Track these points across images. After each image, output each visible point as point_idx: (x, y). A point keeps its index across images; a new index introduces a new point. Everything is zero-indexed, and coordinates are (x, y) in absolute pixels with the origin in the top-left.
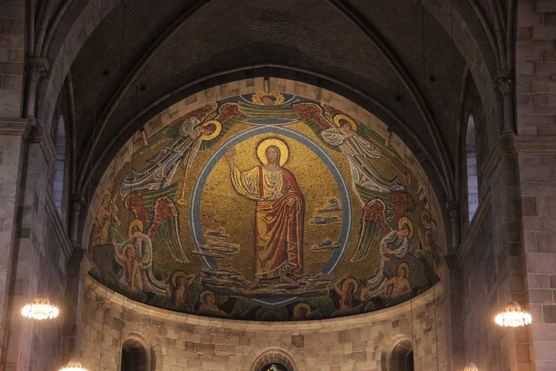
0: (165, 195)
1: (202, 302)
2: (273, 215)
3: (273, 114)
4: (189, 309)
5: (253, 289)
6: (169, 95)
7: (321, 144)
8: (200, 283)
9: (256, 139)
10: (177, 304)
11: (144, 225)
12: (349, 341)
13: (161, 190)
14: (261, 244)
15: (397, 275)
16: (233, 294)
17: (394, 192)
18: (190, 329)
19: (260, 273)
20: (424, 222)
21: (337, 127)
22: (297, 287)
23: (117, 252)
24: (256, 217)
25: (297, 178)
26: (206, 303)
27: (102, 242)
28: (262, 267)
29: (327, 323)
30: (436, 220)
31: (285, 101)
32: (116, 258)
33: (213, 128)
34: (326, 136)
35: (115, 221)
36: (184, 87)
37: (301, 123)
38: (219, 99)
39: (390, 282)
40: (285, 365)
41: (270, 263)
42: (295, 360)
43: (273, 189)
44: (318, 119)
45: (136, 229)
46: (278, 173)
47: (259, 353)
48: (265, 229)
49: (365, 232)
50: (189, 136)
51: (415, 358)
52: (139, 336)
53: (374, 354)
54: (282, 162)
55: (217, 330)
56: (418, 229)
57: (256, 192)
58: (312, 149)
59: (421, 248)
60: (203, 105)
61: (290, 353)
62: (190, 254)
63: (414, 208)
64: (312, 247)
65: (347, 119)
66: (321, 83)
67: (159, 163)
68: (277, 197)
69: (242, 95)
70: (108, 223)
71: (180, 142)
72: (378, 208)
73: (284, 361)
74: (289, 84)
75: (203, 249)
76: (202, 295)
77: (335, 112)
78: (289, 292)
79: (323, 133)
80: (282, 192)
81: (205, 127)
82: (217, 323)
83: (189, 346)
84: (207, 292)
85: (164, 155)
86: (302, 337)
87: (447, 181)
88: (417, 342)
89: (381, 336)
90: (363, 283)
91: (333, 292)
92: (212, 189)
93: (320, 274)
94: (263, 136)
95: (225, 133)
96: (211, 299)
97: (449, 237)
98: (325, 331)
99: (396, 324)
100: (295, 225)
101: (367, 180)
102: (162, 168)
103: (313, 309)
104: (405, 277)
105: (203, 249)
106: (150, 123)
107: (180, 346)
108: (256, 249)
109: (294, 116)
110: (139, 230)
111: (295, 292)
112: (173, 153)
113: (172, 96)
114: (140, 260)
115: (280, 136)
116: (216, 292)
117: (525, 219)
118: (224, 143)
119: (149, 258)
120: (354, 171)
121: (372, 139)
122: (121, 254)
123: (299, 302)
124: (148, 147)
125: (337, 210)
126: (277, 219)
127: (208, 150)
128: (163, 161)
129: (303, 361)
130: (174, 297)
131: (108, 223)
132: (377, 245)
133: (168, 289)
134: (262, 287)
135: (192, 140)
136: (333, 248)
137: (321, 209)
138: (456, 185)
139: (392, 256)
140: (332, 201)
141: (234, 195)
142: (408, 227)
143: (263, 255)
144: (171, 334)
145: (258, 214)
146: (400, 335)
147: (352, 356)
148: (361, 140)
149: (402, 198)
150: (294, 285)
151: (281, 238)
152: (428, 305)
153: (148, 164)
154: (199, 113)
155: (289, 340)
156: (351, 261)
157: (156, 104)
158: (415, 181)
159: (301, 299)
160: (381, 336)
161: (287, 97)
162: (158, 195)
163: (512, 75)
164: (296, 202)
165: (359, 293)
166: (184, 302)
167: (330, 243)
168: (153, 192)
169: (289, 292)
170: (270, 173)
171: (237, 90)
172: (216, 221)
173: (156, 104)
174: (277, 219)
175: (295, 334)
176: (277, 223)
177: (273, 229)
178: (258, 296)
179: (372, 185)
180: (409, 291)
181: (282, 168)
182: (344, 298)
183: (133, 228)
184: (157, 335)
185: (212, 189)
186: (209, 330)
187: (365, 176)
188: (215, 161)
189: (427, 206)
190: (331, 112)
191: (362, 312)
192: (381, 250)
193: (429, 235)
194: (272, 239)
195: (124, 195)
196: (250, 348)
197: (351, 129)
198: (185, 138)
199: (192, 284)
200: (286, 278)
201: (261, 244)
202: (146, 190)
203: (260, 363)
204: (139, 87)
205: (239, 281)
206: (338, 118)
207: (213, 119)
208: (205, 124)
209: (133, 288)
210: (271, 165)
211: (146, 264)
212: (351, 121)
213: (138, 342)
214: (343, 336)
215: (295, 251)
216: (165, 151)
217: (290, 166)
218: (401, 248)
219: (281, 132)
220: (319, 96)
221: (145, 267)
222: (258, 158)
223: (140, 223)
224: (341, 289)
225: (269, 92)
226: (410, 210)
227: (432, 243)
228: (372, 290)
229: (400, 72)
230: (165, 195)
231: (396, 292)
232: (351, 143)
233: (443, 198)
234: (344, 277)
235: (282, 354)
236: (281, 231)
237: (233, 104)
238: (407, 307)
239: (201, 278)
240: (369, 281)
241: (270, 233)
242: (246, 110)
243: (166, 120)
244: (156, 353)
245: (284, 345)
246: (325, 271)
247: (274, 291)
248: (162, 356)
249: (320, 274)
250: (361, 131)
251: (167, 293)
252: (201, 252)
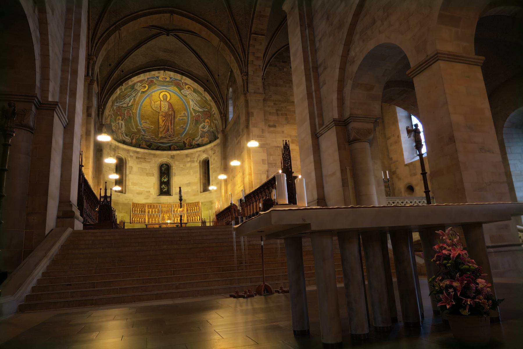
0: (128, 109)
1: (141, 144)
2: (164, 117)
3: (166, 84)
4: (137, 146)
5: (158, 140)
6: (131, 74)
7: (181, 95)
8: (141, 138)
9: (160, 91)
10: (133, 145)
11: (122, 118)
12: (189, 157)
13: (127, 107)
15: (204, 137)
16: (151, 142)
17: (204, 111)
18: (138, 153)
19: (160, 135)
20: (214, 121)
21: (186, 89)
22: (172, 140)
23: (113, 127)
24: (159, 117)
25: (172, 105)
26: (143, 144)
27: (108, 123)
28: (161, 133)
29: (182, 151)
30: (218, 120)
31: (170, 79)
32: (113, 129)
33: (145, 87)
34: (183, 92)
35: (112, 116)
36: (137, 72)
37: (175, 87)
38: (148, 77)
39: (202, 139)
40: (168, 164)
41: (163, 132)
42: (172, 163)
43: (164, 109)
44: (180, 86)
45: (119, 119)
46: (166, 103)
47: (160, 160)
49: (194, 123)
50: (137, 89)
51: (210, 162)
52: (120, 154)
53: (197, 161)
54: (168, 100)
55: (146, 153)
56: (212, 123)
57: (159, 109)
58: (178, 96)
59: (212, 128)
60: (143, 79)
61: (170, 161)
62: (137, 129)
63: (211, 116)
64: (177, 128)
65: (190, 87)
66: (183, 74)
67: (127, 98)
68: (166, 111)
69: (156, 77)
70: (110, 117)
71: (134, 91)
72: (199, 116)
73: (168, 163)
74: (172, 74)
75: (141, 127)
76: (141, 142)
77: (186, 84)
78: (169, 142)
79: (182, 91)
80: (167, 110)
81: (143, 87)
82: (146, 151)
83: (137, 158)
84: (143, 141)
85: (129, 95)
86: (174, 156)
87: (222, 107)
88: (211, 157)
89: (199, 155)
90: (194, 139)
91: (184, 142)
92: (144, 107)
93: (180, 136)
94: (162, 91)
95: (149, 89)
96: (144, 143)
97: (222, 125)
98: (181, 154)
99: (204, 152)
100: (172, 120)
101: (196, 107)
102: (128, 99)
103: (177, 147)
104: (207, 137)
105: (141, 127)
106: (125, 84)
107: (134, 158)
108: (159, 128)
109: (172, 85)
110: (120, 120)
111: (171, 142)
112: (132, 94)
113: (133, 75)
114: (120, 130)
115: (168, 91)
116: (146, 141)
117: (250, 117)
118: (149, 92)
119: (123, 129)
120: (192, 104)
121: (198, 94)
122: (114, 127)
123: (173, 145)
124: (124, 92)
125: (186, 116)
126: (166, 118)
127: (143, 94)
128: (128, 97)
129: (175, 163)
130: (132, 142)
131: (110, 117)
132: (198, 128)
133: (130, 140)
134: (161, 140)
135: (138, 90)
136: (184, 128)
137: (180, 116)
138: (225, 109)
139: (203, 131)
140: (184, 113)
141: (152, 110)
142: (208, 122)
143: (161, 130)
144: (131, 154)
145: (159, 116)
146: (205, 155)
147: (190, 161)
148: (194, 94)
149: (207, 113)
150: (171, 139)
151: (167, 124)
152: (214, 146)
153: (123, 97)
154: (141, 81)
155: (170, 156)
156: (190, 132)
157: (127, 77)
158: (211, 108)
159: (174, 144)
160: (199, 155)
161: (171, 78)
162: (126, 108)
163: (247, 75)
164: (172, 113)
165: (192, 142)
166: (135, 144)
167: (183, 127)
168: (125, 107)
169: (169, 142)
170: (164, 103)
171: (154, 75)
172: (146, 118)
173: (127, 77)
174: (166, 118)
175: (172, 155)
176: (166, 120)
177: (164, 122)
178: (159, 143)
179: (197, 109)
180: (208, 141)
181: (168, 102)
182: (187, 144)
183: (118, 119)
184: (127, 154)
185: (144, 107)
186: (144, 153)
187: (195, 106)
188: (145, 98)
189: (215, 116)
190: (185, 84)
191: (193, 148)
192: (199, 129)
193: (215, 125)
194: (164, 124)
195: (115, 108)
196: (157, 159)
197: (191, 90)
198: (136, 90)
199: (138, 138)
200: (169, 137)
201: (160, 126)
202: (122, 106)
203: (160, 164)
204: (121, 71)
205: (153, 138)
206: (187, 86)
207: (145, 84)
208: (143, 86)
209: (119, 139)
210: (164, 101)
211: (123, 131)
212: (191, 88)
213: (120, 156)
214: (187, 156)
216: (129, 94)
217: (171, 101)
218: (206, 128)
219: (168, 90)
220: (182, 79)
221: (122, 132)
222: (160, 98)
223: (120, 117)
224: (187, 141)
225: (165, 76)
226: (209, 117)
227: (216, 127)
228: (196, 141)
229: (209, 73)
230: (128, 109)
231: (204, 142)
232: (191, 95)
233: (221, 113)
234: (187, 137)
235: (168, 161)
236: (167, 122)
237: (152, 79)
238: (209, 146)
239: (141, 137)
240: (196, 139)
241: (164, 123)
242: (156, 82)
243: (130, 82)
244: (127, 160)
245: (168, 158)
246: (181, 135)
247: (165, 141)
248: (128, 161)
249: (180, 136)
250: (195, 91)
251: (130, 141)
252: (140, 128)
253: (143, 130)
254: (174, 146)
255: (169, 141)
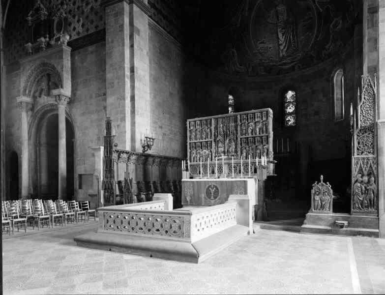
14: (280, 42)
28: (282, 52)
48: (281, 35)
143: (282, 47)
178: (280, 65)
201: (280, 42)
215: (294, 42)
241: (284, 37)
252: (257, 51)
253: (260, 53)
254: (299, 64)
255: (293, 59)
